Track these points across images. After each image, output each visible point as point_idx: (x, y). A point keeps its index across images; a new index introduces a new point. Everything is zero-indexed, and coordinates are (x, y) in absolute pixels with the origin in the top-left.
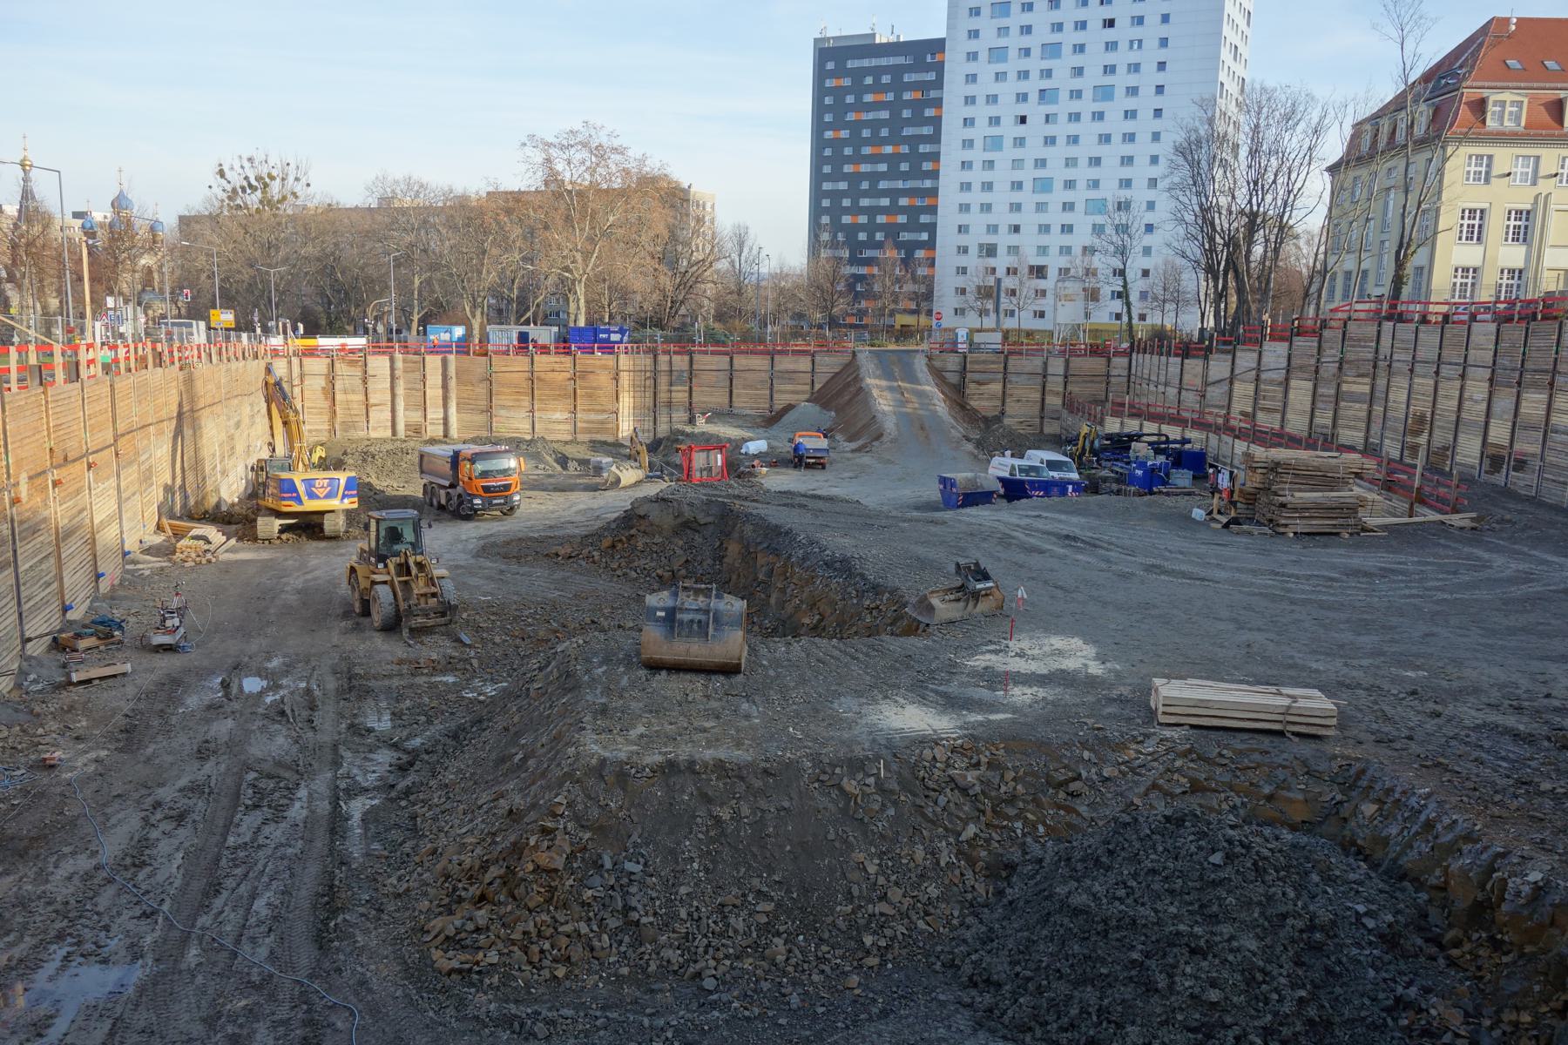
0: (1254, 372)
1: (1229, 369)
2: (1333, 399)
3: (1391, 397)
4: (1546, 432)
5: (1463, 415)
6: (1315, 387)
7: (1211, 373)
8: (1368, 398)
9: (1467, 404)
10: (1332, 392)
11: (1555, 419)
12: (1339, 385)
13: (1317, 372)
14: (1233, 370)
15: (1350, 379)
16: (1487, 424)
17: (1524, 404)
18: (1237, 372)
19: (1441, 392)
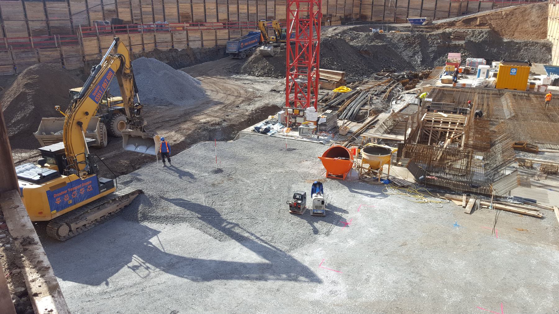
0: (100, 6)
1: (84, 5)
2: (140, 15)
3: (166, 11)
4: (238, 14)
5: (207, 13)
6: (131, 10)
7: (72, 9)
8: (152, 13)
9: (207, 11)
10: (139, 12)
11: (240, 11)
12: (141, 9)
13: (131, 4)
14: (87, 6)
15: (145, 6)
16: (217, 15)
17: (230, 9)
18: (89, 7)
19: (194, 8)
